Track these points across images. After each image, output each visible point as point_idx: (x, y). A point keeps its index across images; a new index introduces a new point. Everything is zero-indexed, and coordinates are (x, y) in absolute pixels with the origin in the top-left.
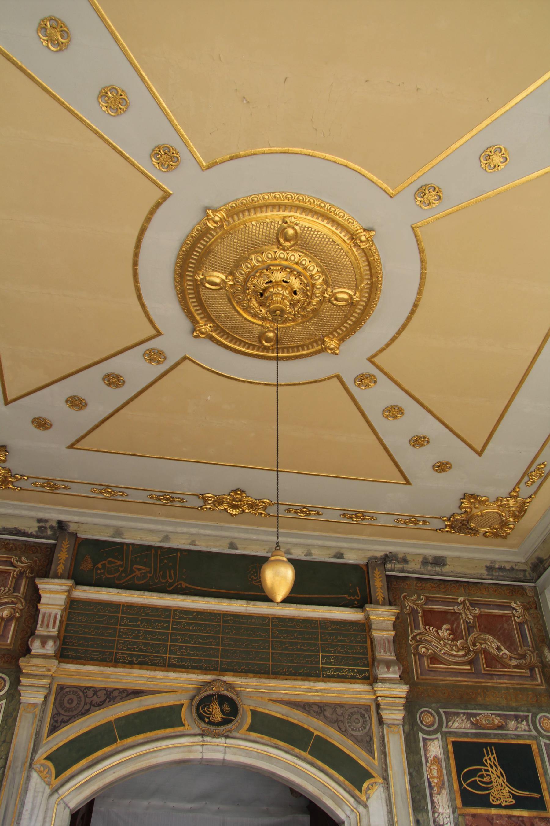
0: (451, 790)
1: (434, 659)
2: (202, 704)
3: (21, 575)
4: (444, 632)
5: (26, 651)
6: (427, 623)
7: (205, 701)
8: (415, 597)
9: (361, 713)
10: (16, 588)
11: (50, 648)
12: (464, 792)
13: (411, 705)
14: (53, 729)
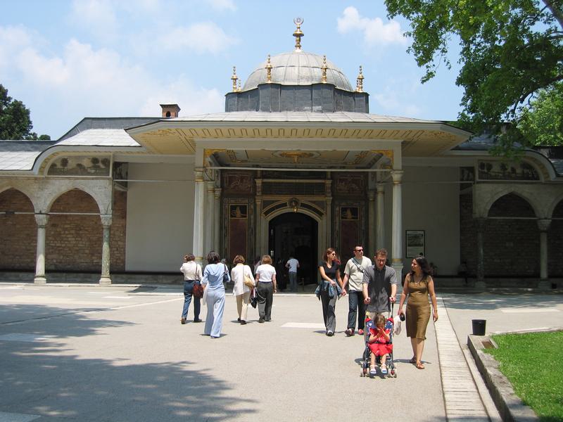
1: (340, 190)
2: (291, 202)
5: (256, 194)
9: (322, 202)
11: (260, 194)
13: (333, 201)
14: (264, 208)
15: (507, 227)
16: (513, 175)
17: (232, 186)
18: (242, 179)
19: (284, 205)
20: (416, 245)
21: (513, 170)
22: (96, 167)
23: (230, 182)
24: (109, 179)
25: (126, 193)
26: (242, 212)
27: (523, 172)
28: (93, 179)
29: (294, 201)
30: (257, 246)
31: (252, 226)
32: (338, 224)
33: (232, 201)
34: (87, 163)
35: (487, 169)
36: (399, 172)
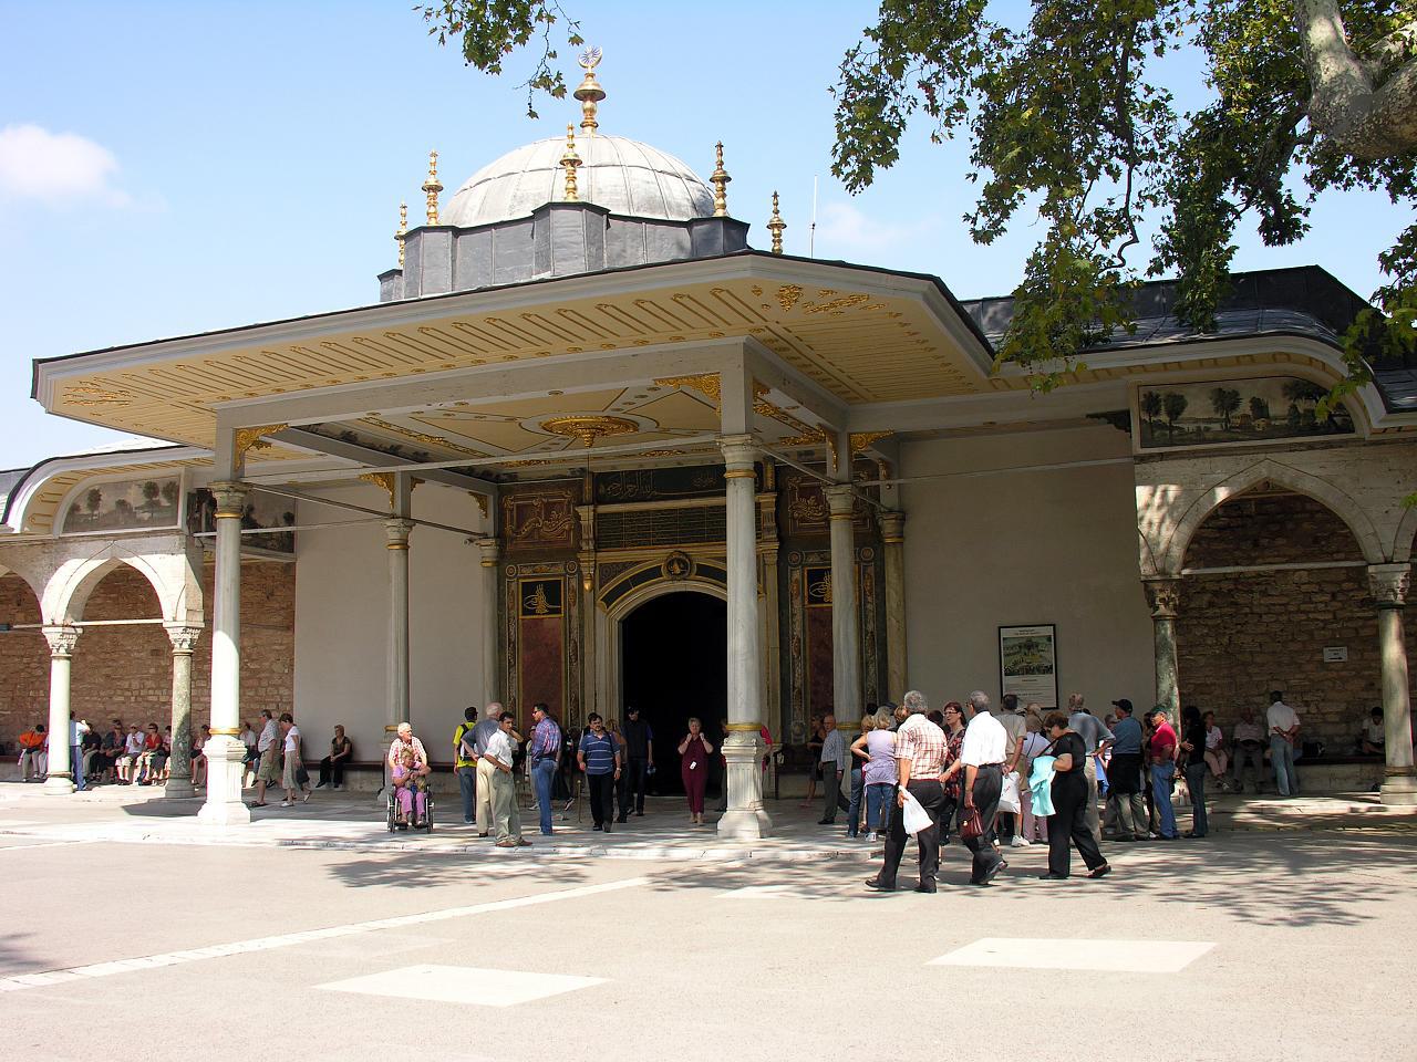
0: (803, 597)
1: (803, 520)
3: (569, 502)
4: (811, 501)
6: (801, 496)
7: (670, 563)
8: (795, 478)
10: (569, 512)
12: (810, 596)
14: (601, 587)
15: (1327, 598)
16: (1260, 423)
17: (525, 530)
18: (549, 507)
19: (654, 573)
20: (1029, 671)
21: (1259, 408)
22: (153, 506)
23: (519, 527)
24: (178, 532)
25: (289, 569)
26: (550, 601)
27: (1294, 407)
28: (148, 534)
29: (679, 561)
30: (589, 689)
31: (575, 635)
32: (798, 618)
33: (527, 572)
34: (135, 497)
35: (1169, 413)
36: (738, 440)
